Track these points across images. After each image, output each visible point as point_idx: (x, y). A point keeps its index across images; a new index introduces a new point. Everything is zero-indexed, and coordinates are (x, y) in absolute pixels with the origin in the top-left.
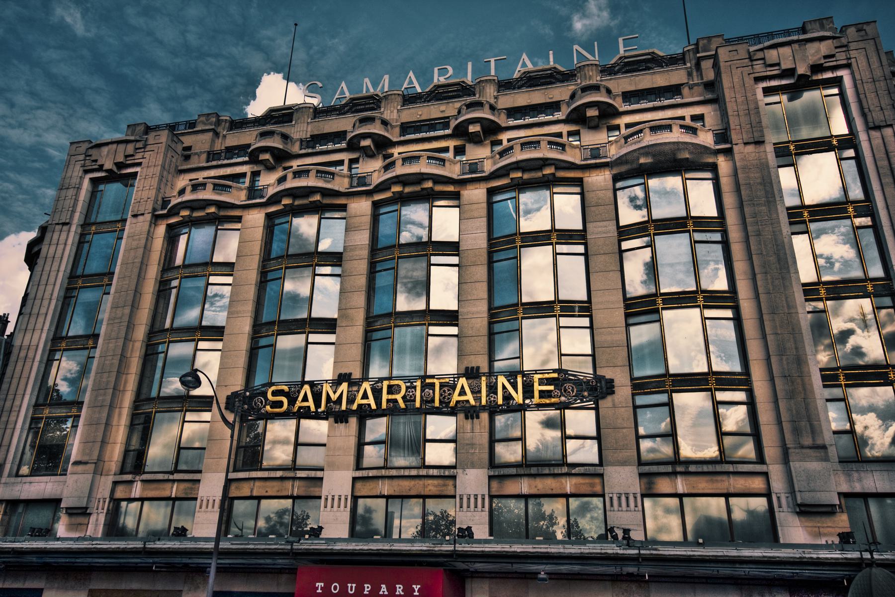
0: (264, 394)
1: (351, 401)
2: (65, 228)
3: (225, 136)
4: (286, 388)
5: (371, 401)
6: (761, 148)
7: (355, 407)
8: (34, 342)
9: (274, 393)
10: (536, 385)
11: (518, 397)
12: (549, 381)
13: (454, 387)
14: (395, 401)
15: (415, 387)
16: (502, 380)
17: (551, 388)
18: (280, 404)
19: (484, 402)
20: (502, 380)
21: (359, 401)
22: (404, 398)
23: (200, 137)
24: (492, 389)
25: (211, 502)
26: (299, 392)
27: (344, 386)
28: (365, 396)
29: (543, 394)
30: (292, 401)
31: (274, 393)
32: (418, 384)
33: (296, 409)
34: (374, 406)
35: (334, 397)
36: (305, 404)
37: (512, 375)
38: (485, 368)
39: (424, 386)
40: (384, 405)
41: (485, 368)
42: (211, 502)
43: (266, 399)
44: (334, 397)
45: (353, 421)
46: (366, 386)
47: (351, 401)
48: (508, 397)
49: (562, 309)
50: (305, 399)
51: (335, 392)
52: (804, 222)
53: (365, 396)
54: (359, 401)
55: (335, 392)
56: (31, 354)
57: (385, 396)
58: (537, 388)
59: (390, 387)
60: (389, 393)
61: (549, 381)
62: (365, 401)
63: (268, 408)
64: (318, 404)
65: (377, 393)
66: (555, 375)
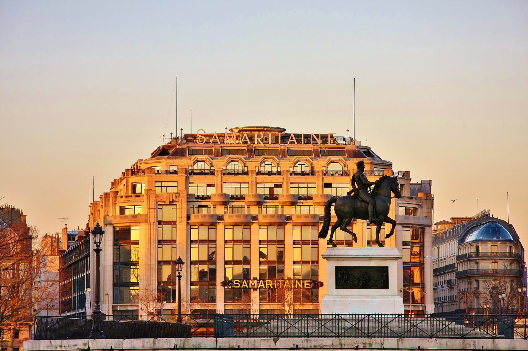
0: (233, 282)
1: (258, 285)
2: (154, 223)
3: (188, 177)
5: (263, 285)
6: (364, 224)
7: (259, 287)
8: (154, 263)
9: (236, 282)
10: (305, 283)
11: (301, 286)
12: (308, 283)
13: (285, 283)
14: (269, 286)
15: (274, 282)
16: (297, 282)
17: (309, 284)
18: (238, 285)
19: (292, 287)
20: (297, 282)
21: (260, 285)
22: (272, 285)
23: (180, 178)
24: (294, 283)
25: (220, 310)
26: (243, 282)
27: (255, 282)
28: (261, 284)
29: (307, 286)
30: (241, 285)
31: (236, 282)
32: (276, 281)
34: (264, 287)
35: (253, 284)
36: (245, 286)
37: (299, 281)
38: (292, 278)
39: (277, 282)
40: (267, 287)
41: (292, 278)
42: (220, 310)
43: (233, 284)
44: (253, 284)
45: (258, 290)
46: (261, 281)
47: (258, 285)
48: (298, 286)
49: (312, 263)
50: (245, 284)
51: (253, 283)
52: (370, 245)
53: (261, 284)
54: (260, 285)
55: (253, 283)
56: (154, 267)
57: (267, 285)
58: (305, 284)
59: (268, 282)
60: (268, 283)
61: (308, 283)
62: (261, 286)
63: (234, 286)
65: (265, 284)
66: (310, 281)
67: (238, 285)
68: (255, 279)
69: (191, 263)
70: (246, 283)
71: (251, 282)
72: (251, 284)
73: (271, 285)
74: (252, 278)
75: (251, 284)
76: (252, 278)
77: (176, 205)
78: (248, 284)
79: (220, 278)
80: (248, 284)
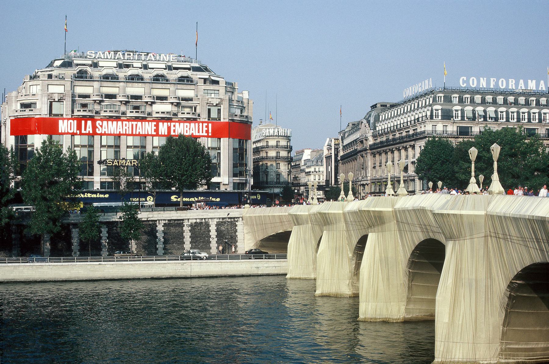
0: (106, 161)
1: (126, 164)
4: (111, 160)
9: (109, 161)
18: (110, 164)
30: (113, 163)
31: (109, 161)
33: (114, 165)
35: (122, 163)
36: (116, 164)
47: (126, 164)
50: (116, 163)
57: (133, 163)
64: (119, 164)
67: (110, 164)
68: (123, 159)
69: (74, 146)
70: (117, 162)
71: (120, 161)
72: (121, 163)
73: (135, 164)
74: (121, 158)
75: (121, 163)
76: (121, 158)
77: (63, 102)
78: (118, 162)
79: (96, 159)
80: (118, 162)
